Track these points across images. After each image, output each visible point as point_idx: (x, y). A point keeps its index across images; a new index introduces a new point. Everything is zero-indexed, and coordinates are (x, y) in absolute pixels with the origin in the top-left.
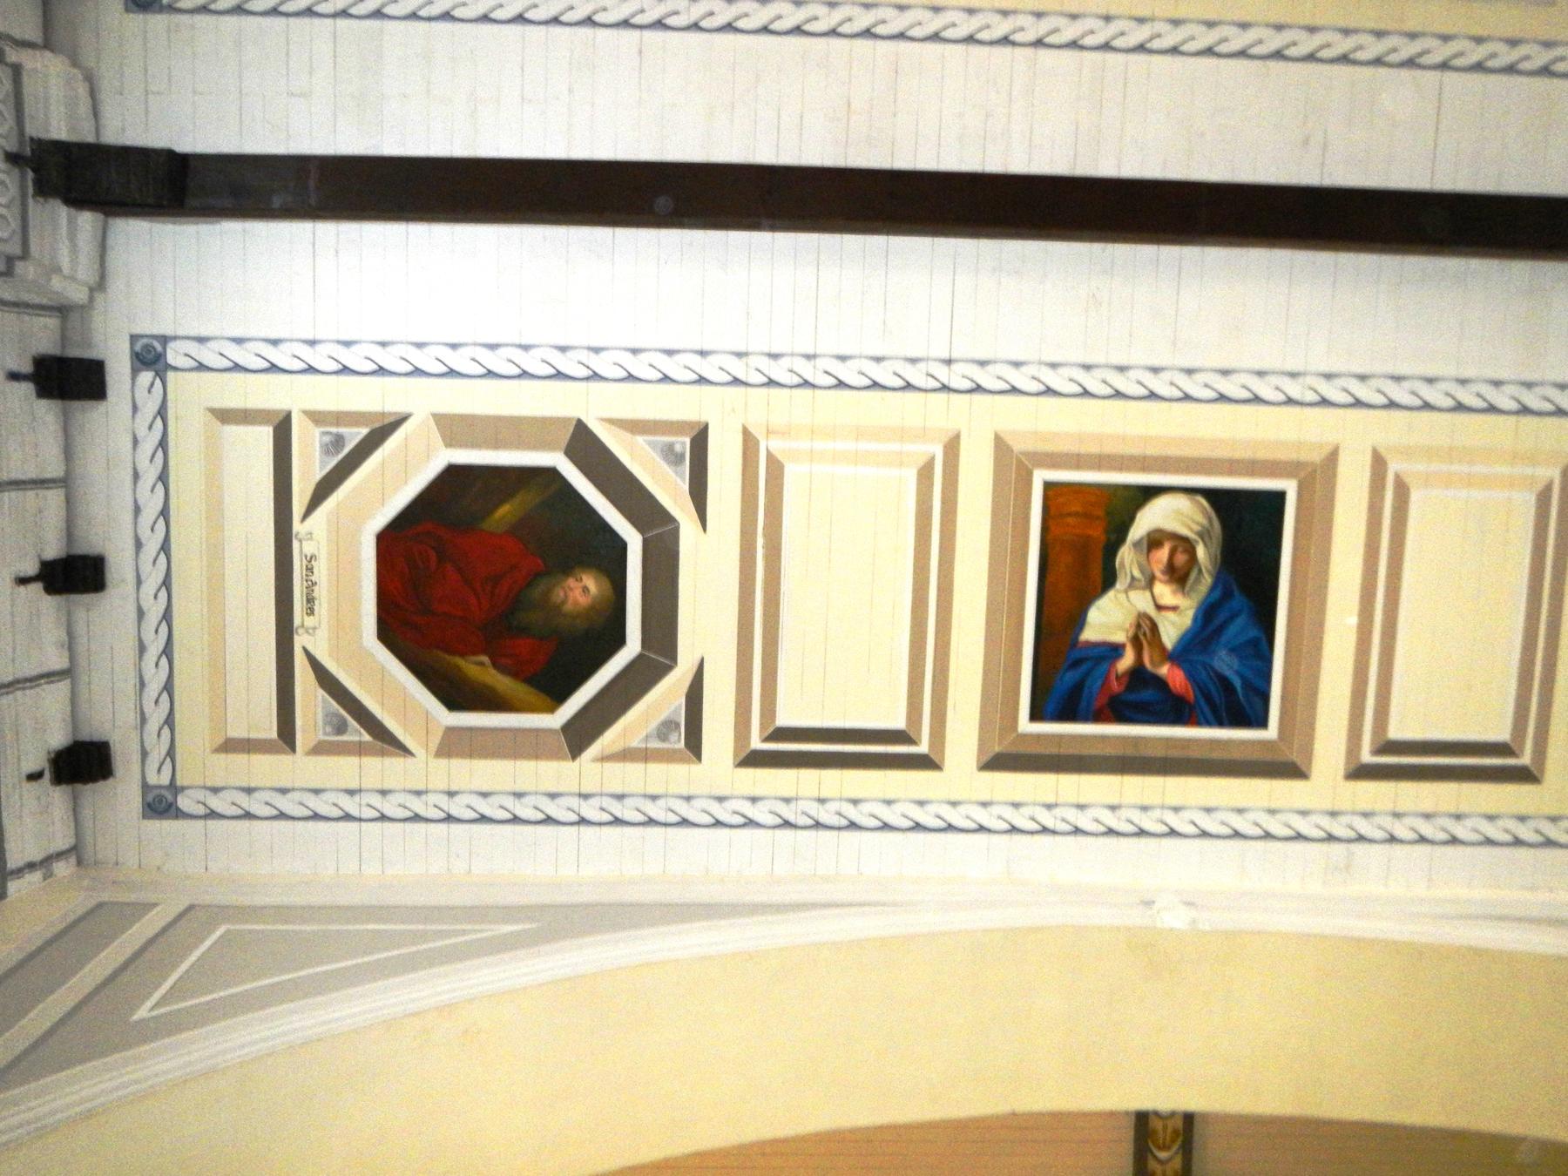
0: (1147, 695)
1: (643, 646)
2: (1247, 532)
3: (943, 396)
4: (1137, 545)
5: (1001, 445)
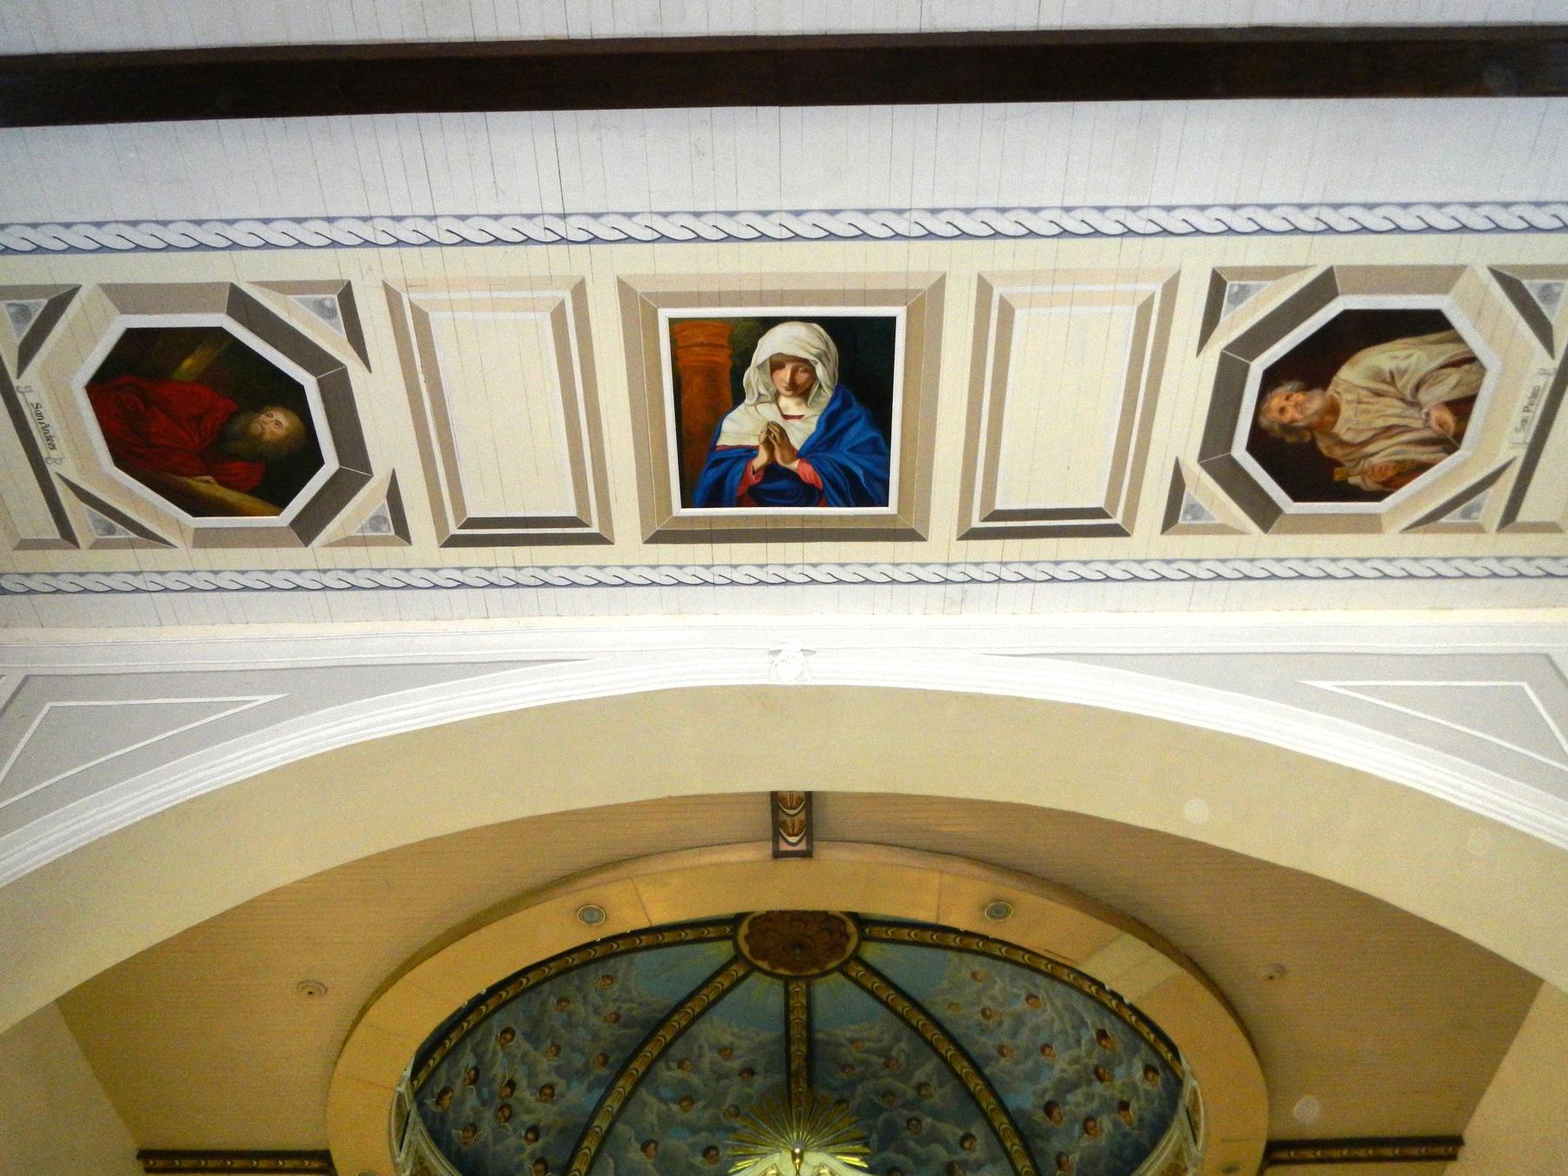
0: (782, 484)
1: (341, 462)
2: (862, 354)
3: (563, 247)
4: (761, 367)
5: (624, 289)
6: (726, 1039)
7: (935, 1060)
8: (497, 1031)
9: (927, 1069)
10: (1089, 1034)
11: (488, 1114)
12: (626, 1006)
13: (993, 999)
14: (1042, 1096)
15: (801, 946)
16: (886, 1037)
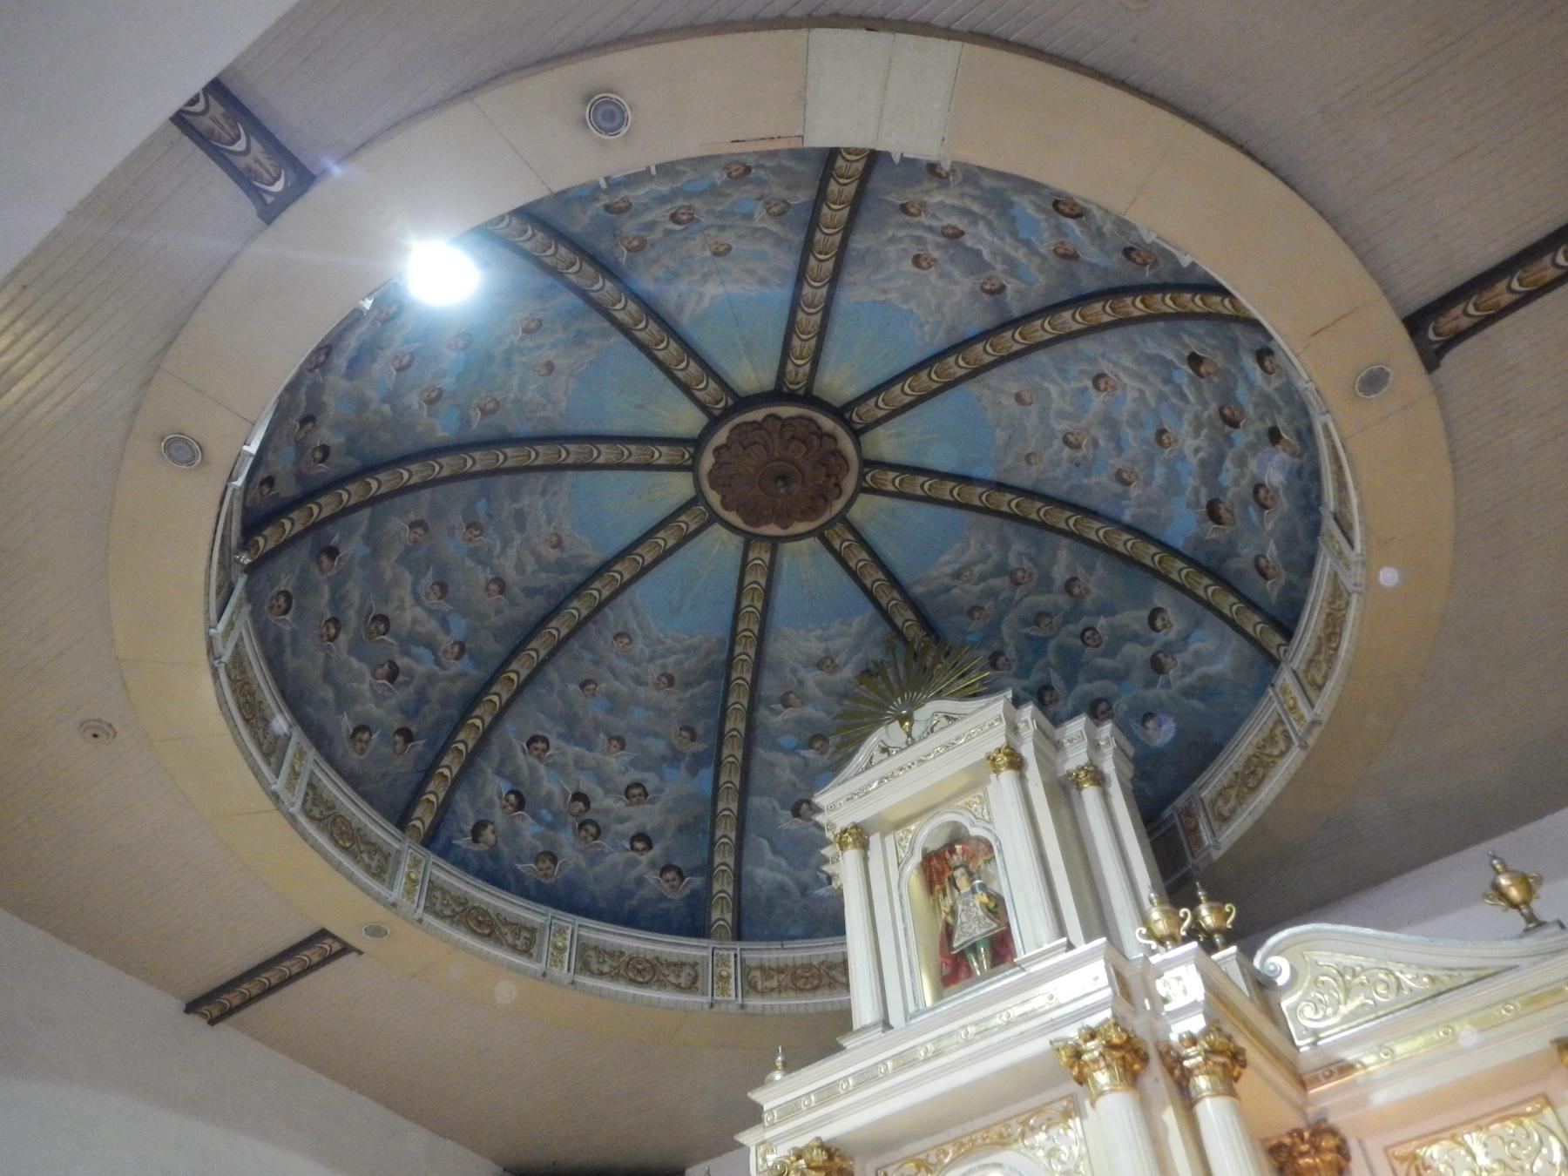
6: (816, 649)
7: (1065, 541)
8: (519, 745)
9: (1063, 560)
10: (1184, 372)
11: (566, 841)
12: (671, 660)
13: (1062, 415)
14: (1197, 504)
15: (784, 478)
16: (991, 547)
